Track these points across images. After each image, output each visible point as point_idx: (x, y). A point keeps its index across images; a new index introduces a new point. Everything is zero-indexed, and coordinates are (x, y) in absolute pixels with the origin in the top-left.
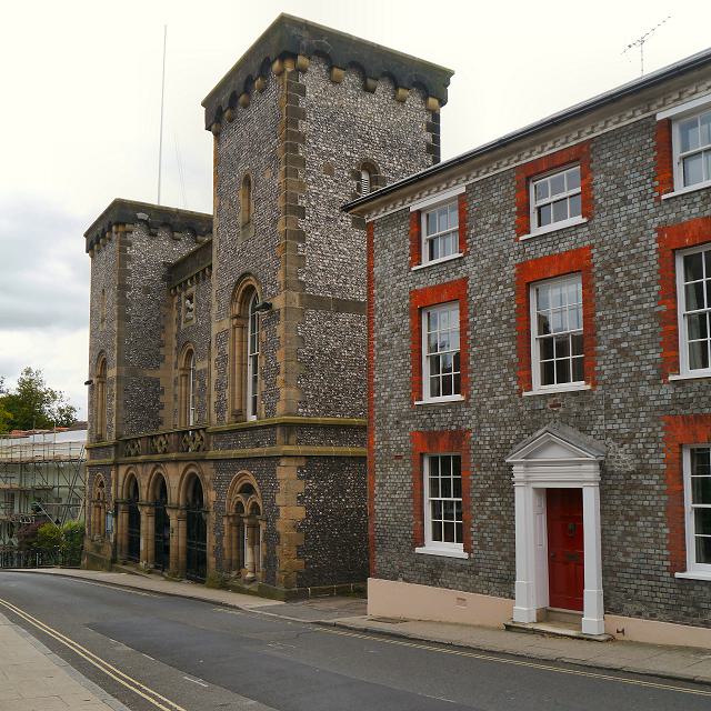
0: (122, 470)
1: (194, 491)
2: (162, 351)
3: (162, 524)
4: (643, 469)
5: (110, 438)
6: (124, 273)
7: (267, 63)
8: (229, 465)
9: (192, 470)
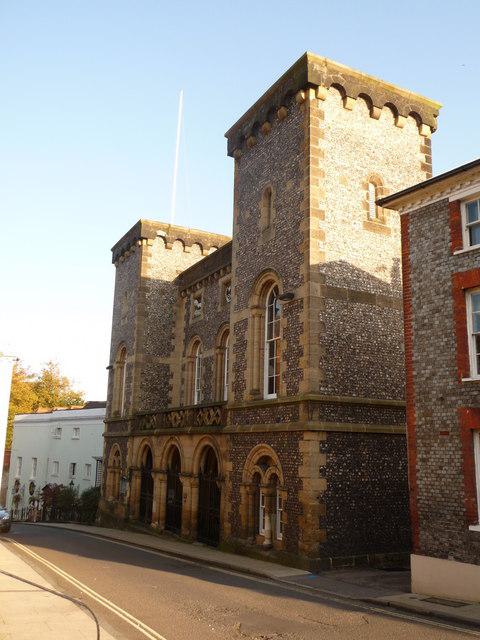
1: (147, 457)
2: (173, 342)
3: (174, 486)
8: (247, 438)
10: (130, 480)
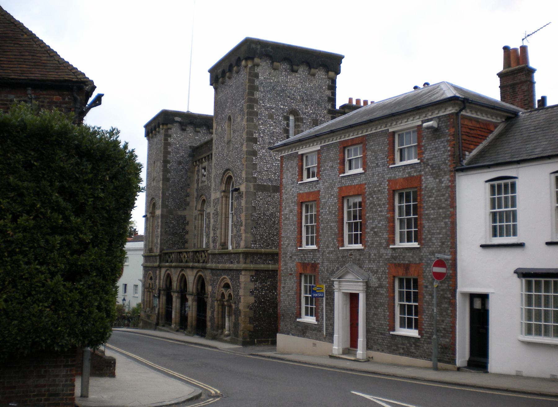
0: (163, 271)
2: (188, 199)
4: (381, 286)
5: (157, 251)
6: (166, 153)
7: (239, 61)
9: (200, 273)
10: (159, 297)
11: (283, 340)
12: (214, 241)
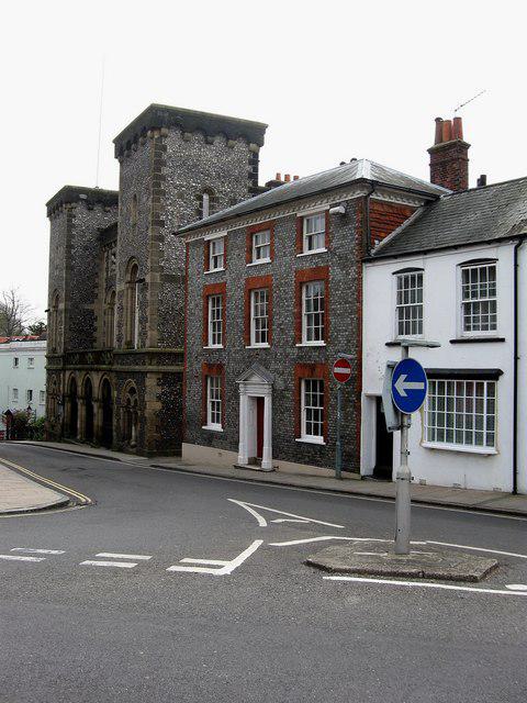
0: (68, 373)
2: (96, 291)
4: (286, 389)
5: (60, 351)
6: (70, 237)
7: (144, 131)
9: (105, 377)
10: (63, 404)
11: (187, 449)
12: (119, 340)
